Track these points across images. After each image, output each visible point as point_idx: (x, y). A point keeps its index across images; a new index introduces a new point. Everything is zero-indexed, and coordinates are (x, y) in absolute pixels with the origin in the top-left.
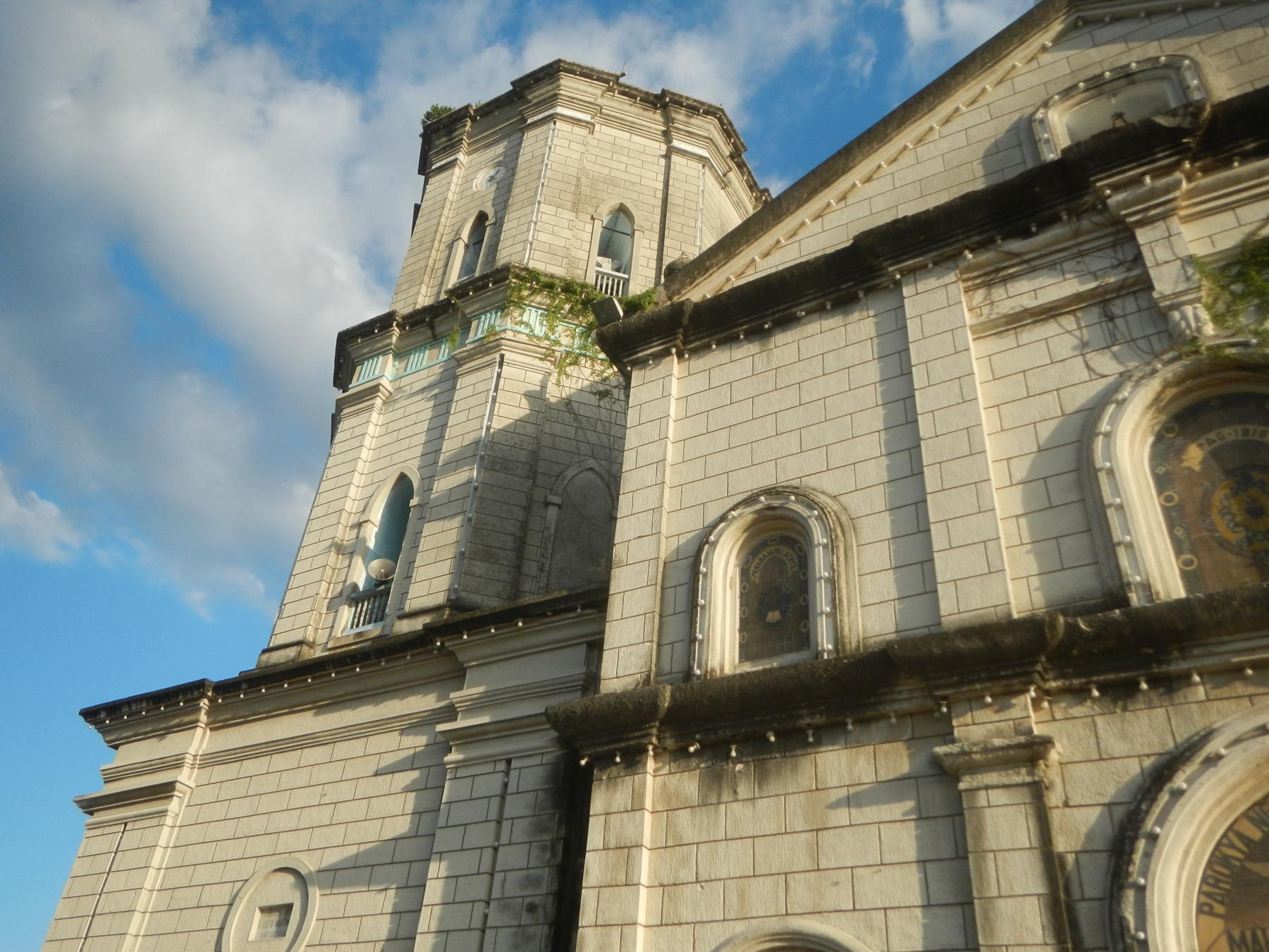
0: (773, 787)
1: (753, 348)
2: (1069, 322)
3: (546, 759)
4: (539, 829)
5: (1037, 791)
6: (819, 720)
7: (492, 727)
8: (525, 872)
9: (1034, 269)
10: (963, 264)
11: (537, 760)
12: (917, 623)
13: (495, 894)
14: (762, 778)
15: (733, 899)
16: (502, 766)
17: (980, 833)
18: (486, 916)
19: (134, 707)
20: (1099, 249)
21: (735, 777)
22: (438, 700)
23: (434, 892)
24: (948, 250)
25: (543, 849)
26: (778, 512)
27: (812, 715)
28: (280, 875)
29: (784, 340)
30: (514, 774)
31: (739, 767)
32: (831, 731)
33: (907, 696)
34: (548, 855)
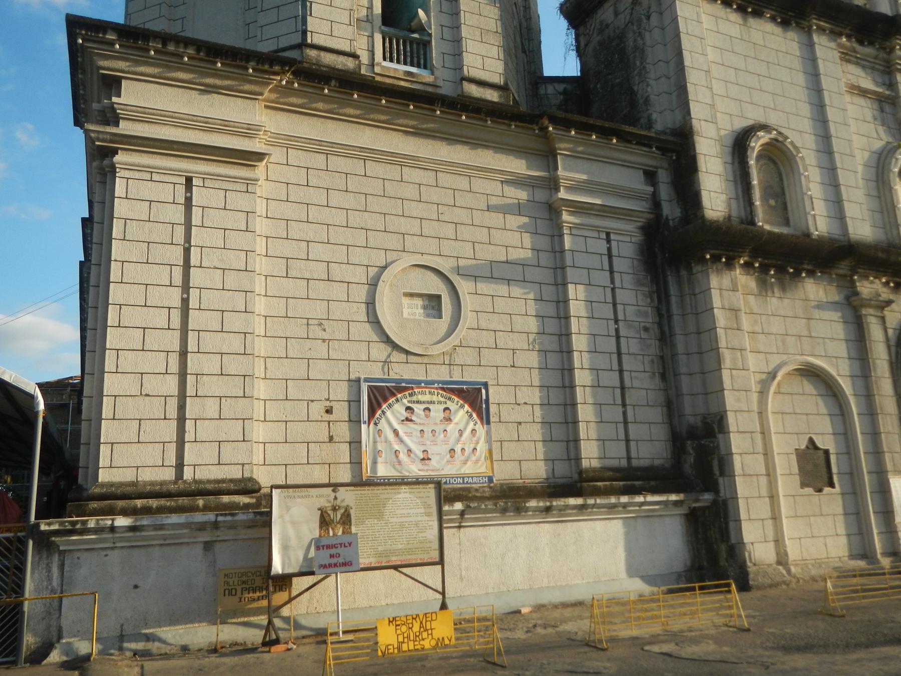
0: (789, 295)
1: (735, 17)
2: (869, 101)
3: (634, 240)
4: (639, 283)
5: (883, 319)
6: (810, 267)
7: (598, 207)
8: (636, 308)
9: (857, 64)
10: (839, 41)
11: (628, 239)
12: (836, 232)
13: (621, 316)
14: (783, 289)
15: (780, 344)
16: (604, 236)
17: (869, 330)
18: (617, 330)
19: (171, 47)
20: (878, 70)
21: (772, 284)
22: (528, 168)
23: (577, 308)
24: (838, 29)
25: (645, 295)
26: (779, 144)
27: (808, 264)
28: (418, 270)
29: (753, 22)
30: (614, 244)
31: (773, 280)
32: (811, 273)
33: (843, 268)
34: (649, 300)
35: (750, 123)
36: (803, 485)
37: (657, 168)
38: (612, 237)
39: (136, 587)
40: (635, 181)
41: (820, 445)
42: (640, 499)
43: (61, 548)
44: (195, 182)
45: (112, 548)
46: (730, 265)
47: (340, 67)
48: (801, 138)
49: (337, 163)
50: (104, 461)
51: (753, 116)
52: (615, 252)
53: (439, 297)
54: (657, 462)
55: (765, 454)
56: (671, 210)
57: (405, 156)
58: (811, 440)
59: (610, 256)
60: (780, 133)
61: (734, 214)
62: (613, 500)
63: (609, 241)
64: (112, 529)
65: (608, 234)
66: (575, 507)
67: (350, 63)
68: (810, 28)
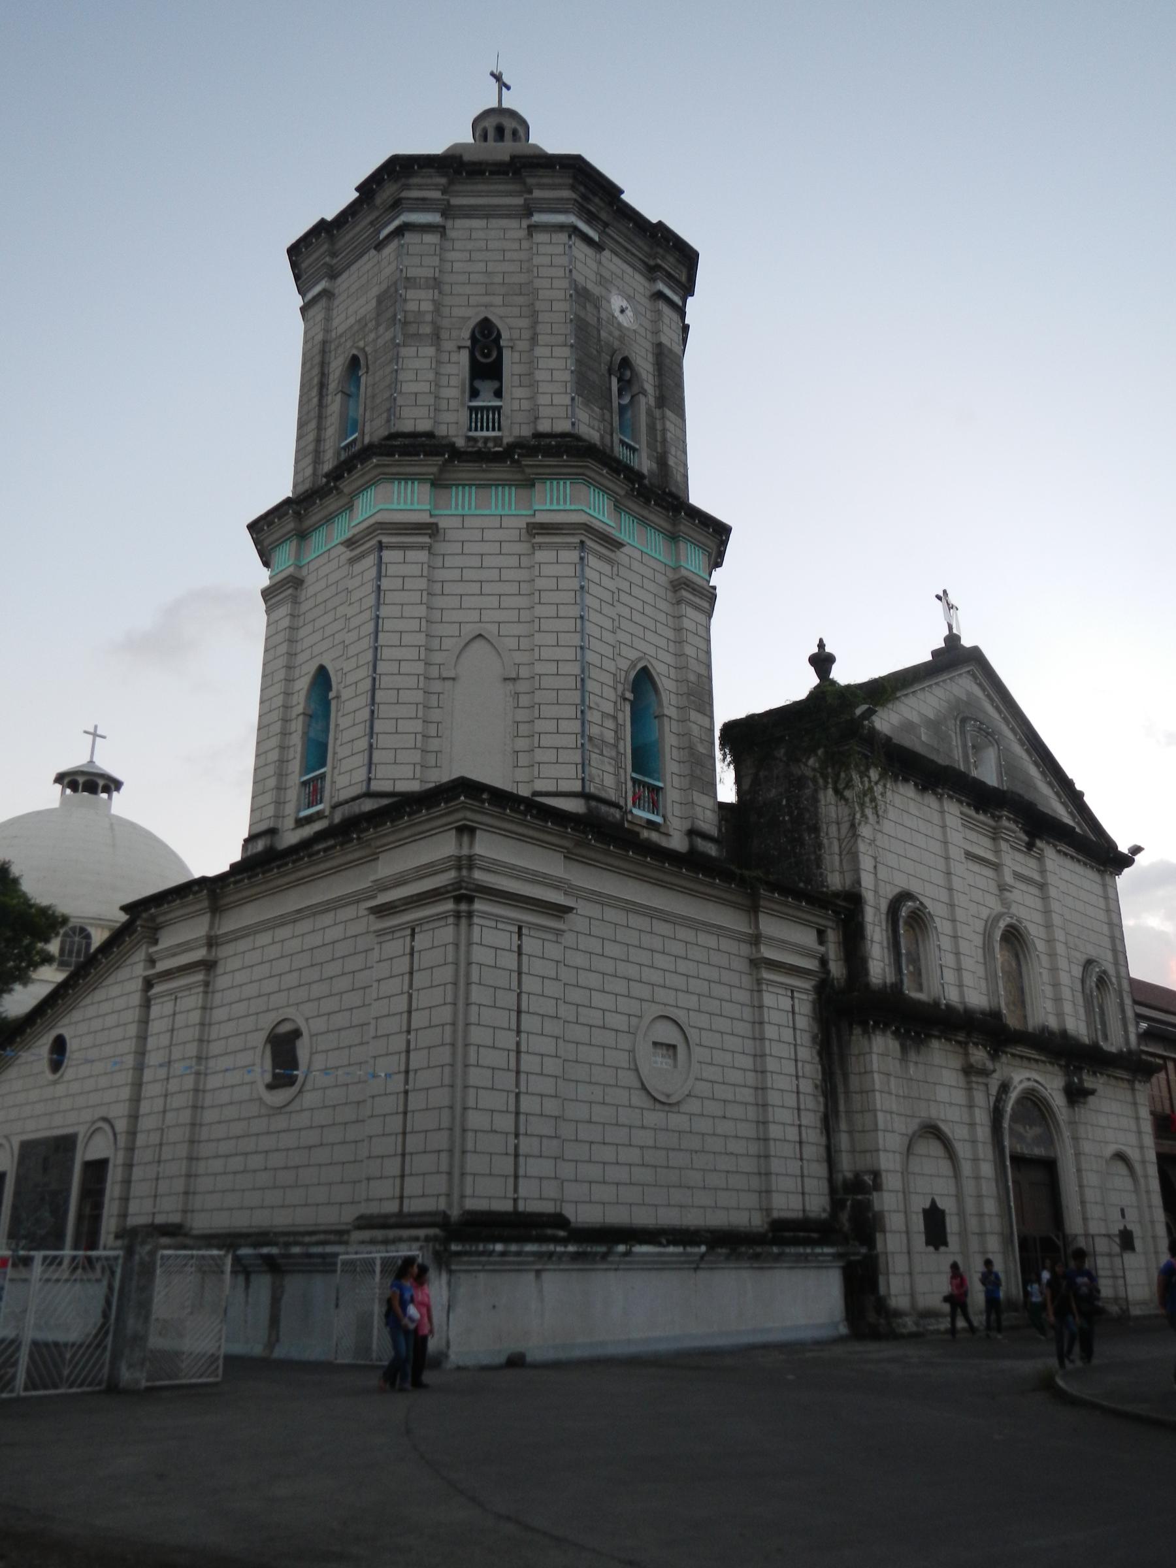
3: (811, 998)
11: (804, 997)
13: (800, 1074)
30: (796, 1001)
35: (897, 890)
36: (928, 1243)
37: (826, 927)
38: (796, 994)
39: (494, 1307)
40: (807, 938)
41: (941, 1204)
42: (818, 1250)
43: (453, 1267)
44: (524, 931)
45: (479, 1271)
46: (884, 1031)
47: (610, 818)
48: (936, 909)
49: (611, 914)
50: (468, 1192)
51: (903, 883)
52: (797, 1009)
53: (674, 1047)
54: (824, 1215)
55: (906, 1212)
56: (837, 969)
57: (656, 910)
58: (933, 1203)
59: (793, 1012)
60: (921, 903)
61: (888, 981)
62: (801, 1250)
63: (792, 998)
64: (491, 1253)
65: (792, 991)
66: (533, 1254)
67: (618, 814)
68: (942, 795)
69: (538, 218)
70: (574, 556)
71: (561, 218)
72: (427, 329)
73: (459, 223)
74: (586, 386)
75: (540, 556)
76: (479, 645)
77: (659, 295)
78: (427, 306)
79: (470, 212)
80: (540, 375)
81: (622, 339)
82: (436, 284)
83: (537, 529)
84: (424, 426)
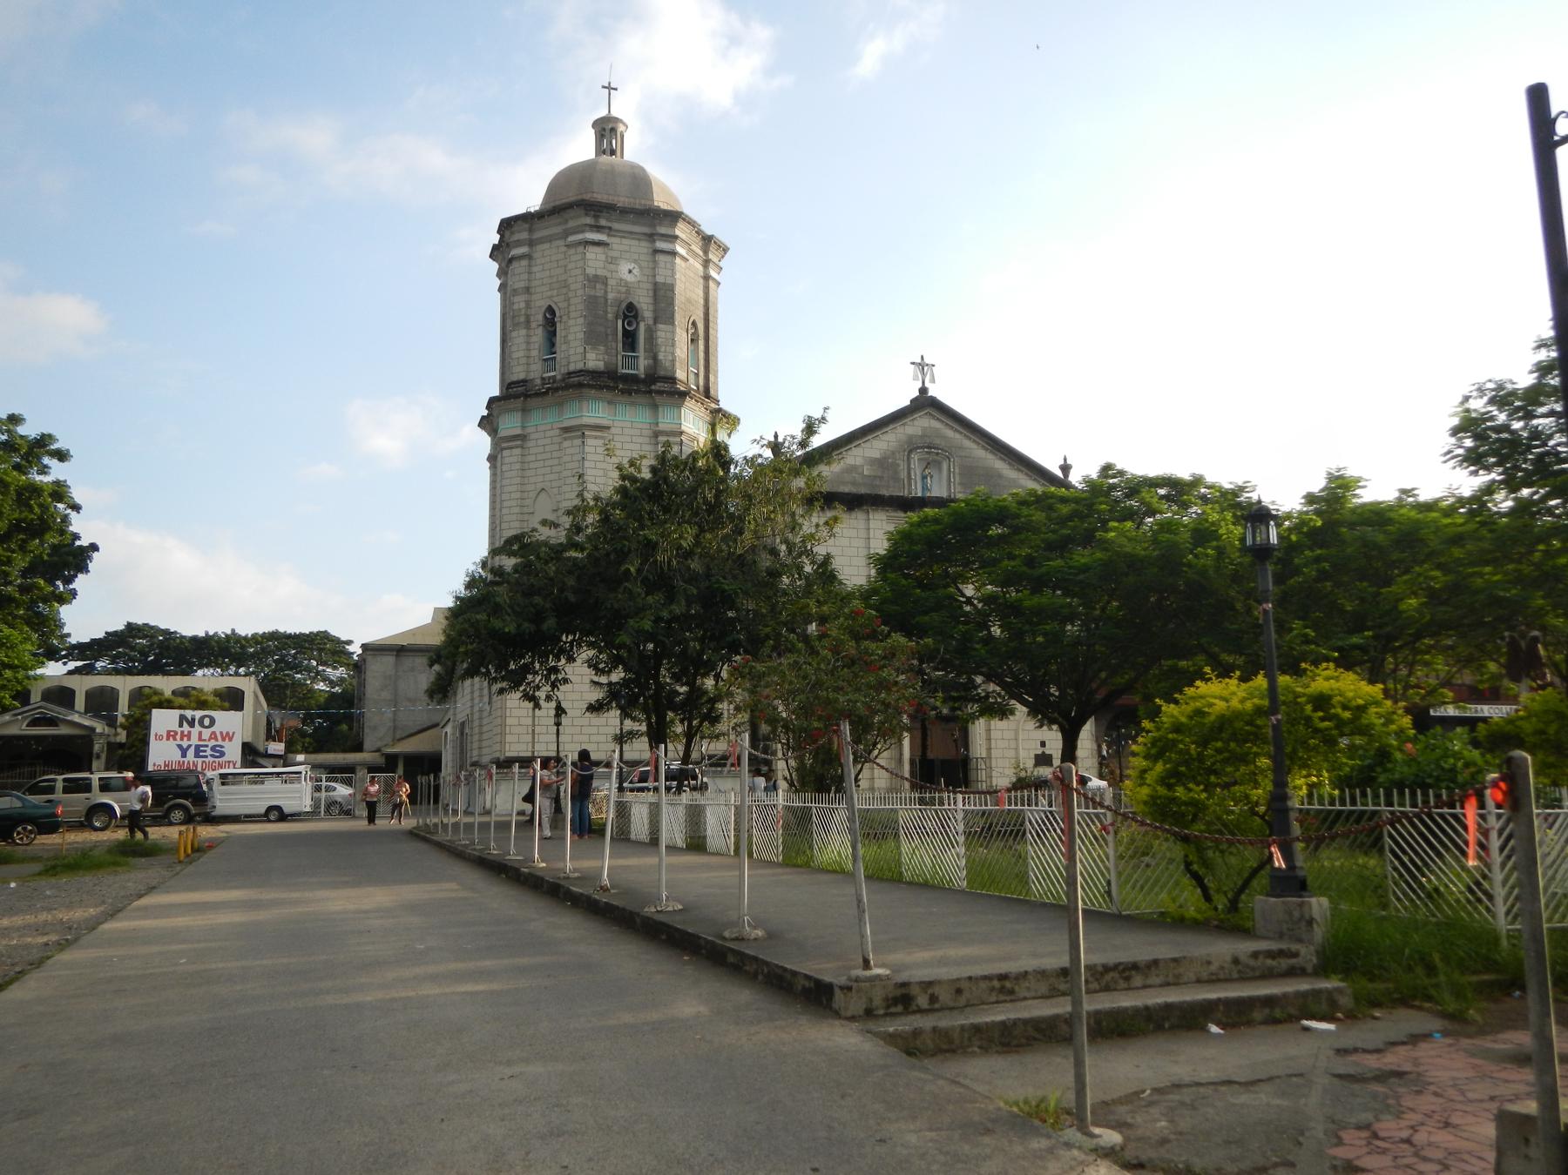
69: (571, 239)
70: (578, 442)
71: (580, 237)
72: (522, 319)
73: (539, 247)
74: (593, 338)
75: (567, 444)
76: (543, 495)
77: (656, 251)
78: (523, 305)
79: (542, 241)
80: (571, 337)
81: (628, 292)
82: (527, 290)
83: (566, 430)
84: (522, 376)
